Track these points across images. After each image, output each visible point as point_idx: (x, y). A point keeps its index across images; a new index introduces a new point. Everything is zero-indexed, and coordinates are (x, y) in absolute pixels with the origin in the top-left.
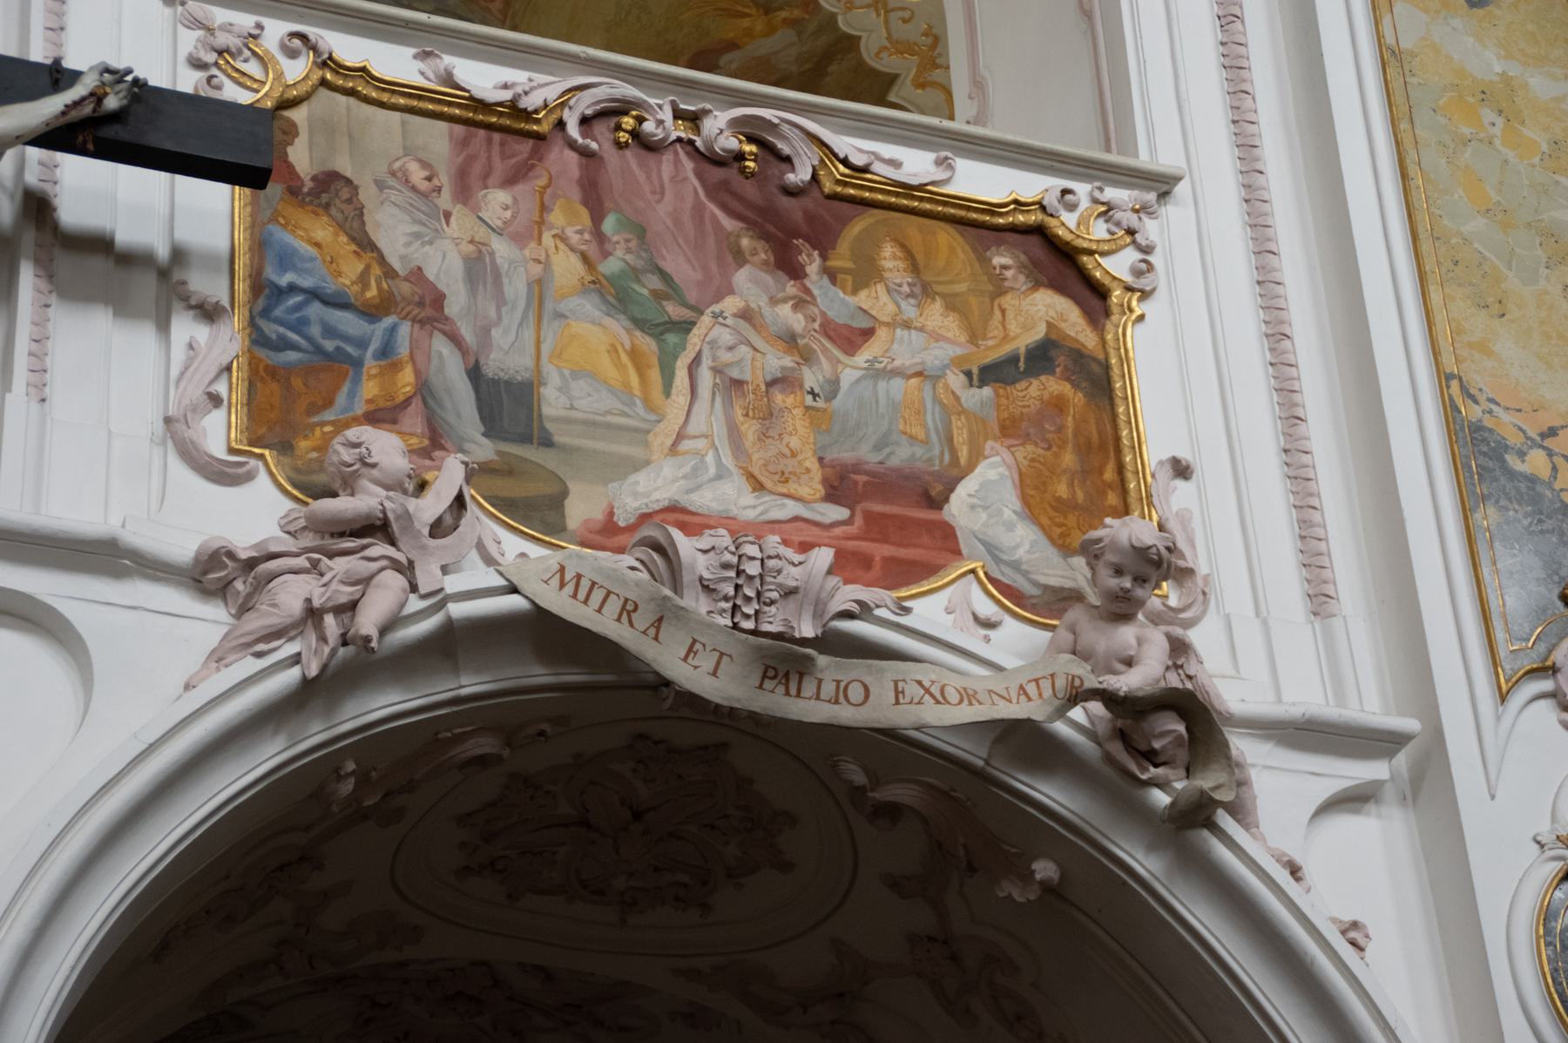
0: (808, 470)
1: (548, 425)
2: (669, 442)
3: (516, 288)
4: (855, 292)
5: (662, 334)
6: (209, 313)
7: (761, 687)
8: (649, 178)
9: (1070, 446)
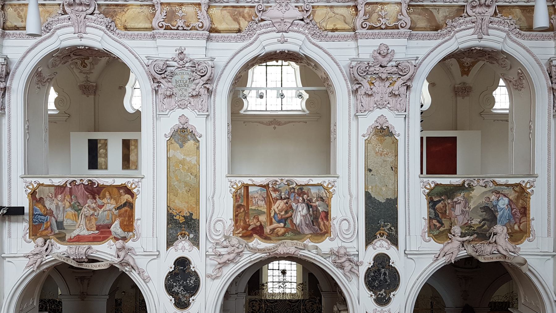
1: (64, 227)
3: (61, 209)
9: (127, 217)
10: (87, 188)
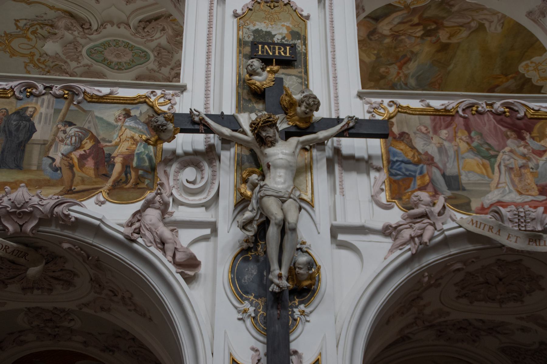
0: (533, 188)
1: (464, 185)
2: (495, 185)
3: (451, 153)
4: (540, 141)
5: (490, 159)
6: (378, 170)
7: (529, 244)
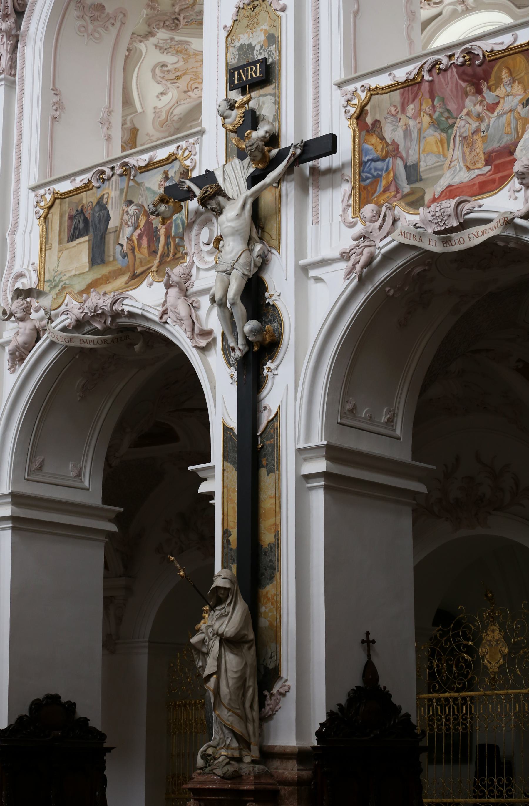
0: (481, 158)
1: (421, 174)
3: (415, 134)
7: (444, 246)
8: (445, 81)
10: (464, 73)
